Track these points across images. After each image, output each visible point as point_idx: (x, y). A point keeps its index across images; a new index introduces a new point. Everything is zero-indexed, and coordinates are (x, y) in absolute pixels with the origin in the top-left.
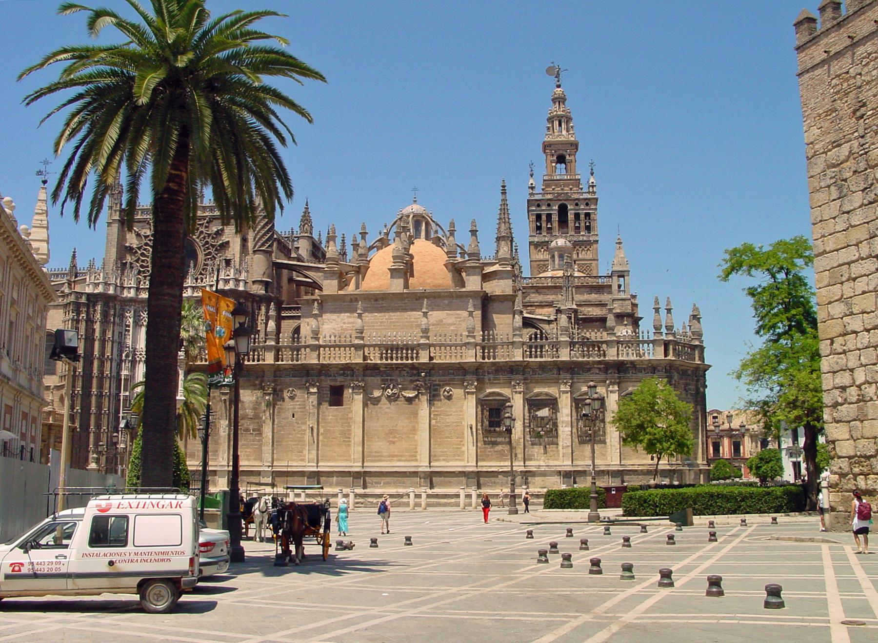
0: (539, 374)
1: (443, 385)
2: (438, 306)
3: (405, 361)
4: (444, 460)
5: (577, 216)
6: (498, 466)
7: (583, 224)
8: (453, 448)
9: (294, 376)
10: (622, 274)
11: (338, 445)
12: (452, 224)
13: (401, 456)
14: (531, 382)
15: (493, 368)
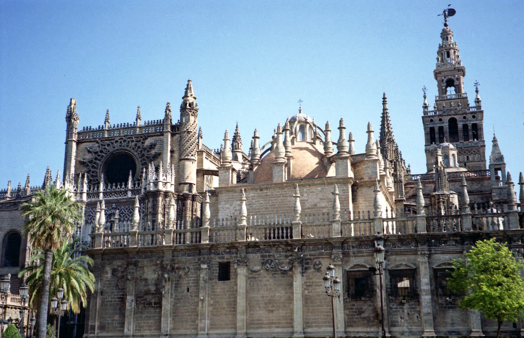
0: (398, 247)
1: (314, 259)
2: (313, 192)
3: (281, 239)
4: (316, 326)
5: (465, 126)
6: (365, 332)
7: (471, 133)
8: (324, 315)
9: (189, 256)
10: (499, 167)
11: (226, 314)
12: (327, 125)
13: (279, 323)
14: (392, 255)
15: (357, 243)
